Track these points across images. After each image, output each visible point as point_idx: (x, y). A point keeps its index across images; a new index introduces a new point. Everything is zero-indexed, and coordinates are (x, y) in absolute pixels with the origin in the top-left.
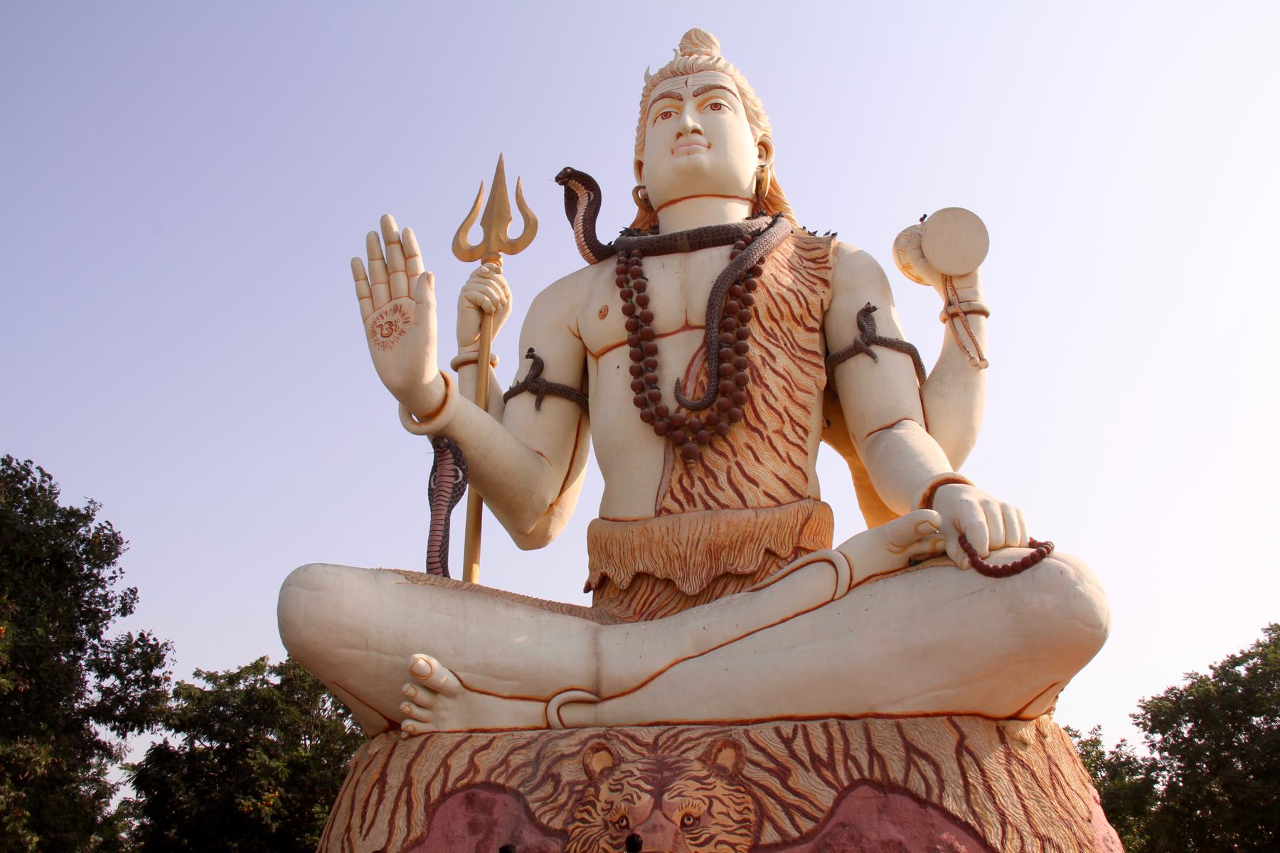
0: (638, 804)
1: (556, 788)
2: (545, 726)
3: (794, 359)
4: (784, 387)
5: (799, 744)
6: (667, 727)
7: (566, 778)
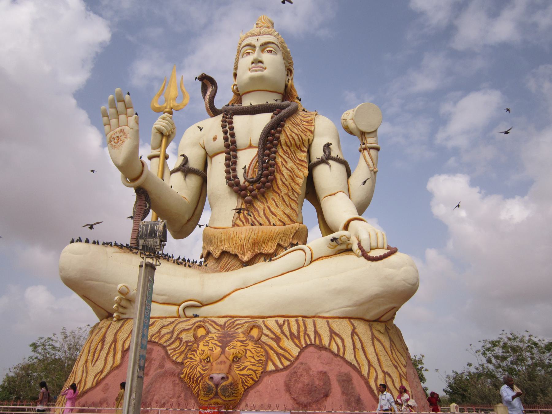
0: (215, 352)
1: (180, 344)
2: (178, 316)
3: (295, 164)
4: (290, 175)
5: (286, 328)
6: (230, 318)
7: (184, 340)
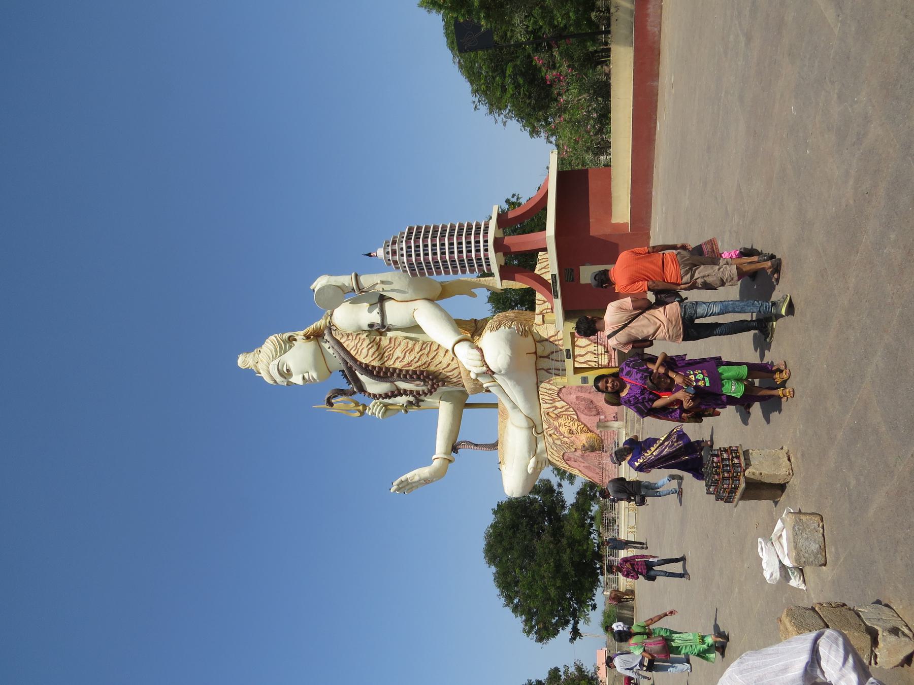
4: (409, 353)
5: (548, 401)
7: (560, 443)
